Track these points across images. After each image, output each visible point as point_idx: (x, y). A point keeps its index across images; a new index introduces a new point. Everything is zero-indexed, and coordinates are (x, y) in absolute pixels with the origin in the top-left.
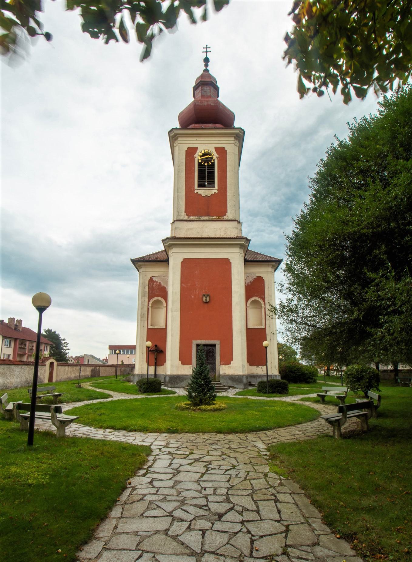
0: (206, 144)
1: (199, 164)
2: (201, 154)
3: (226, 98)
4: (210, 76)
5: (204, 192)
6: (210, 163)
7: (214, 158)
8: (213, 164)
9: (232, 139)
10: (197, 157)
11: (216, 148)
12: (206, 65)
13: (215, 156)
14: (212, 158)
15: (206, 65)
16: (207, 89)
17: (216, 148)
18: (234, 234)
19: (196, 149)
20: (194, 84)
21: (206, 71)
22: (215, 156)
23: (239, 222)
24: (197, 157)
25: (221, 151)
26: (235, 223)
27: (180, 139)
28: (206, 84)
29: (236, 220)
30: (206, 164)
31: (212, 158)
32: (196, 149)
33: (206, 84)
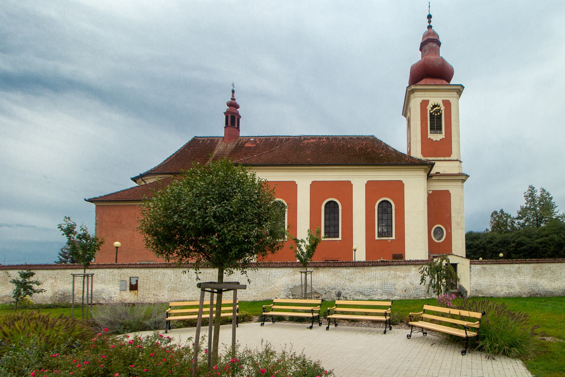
0: (436, 98)
1: (431, 114)
2: (431, 106)
3: (447, 54)
4: (434, 34)
5: (436, 137)
6: (439, 114)
7: (442, 109)
8: (441, 115)
9: (455, 93)
10: (429, 108)
11: (443, 101)
12: (430, 22)
13: (443, 108)
14: (440, 109)
15: (430, 22)
16: (431, 44)
17: (443, 101)
18: (456, 172)
19: (428, 101)
20: (420, 41)
21: (430, 27)
22: (443, 108)
23: (460, 161)
24: (429, 108)
25: (447, 104)
26: (458, 162)
27: (415, 93)
28: (431, 42)
29: (457, 160)
30: (436, 115)
31: (440, 109)
32: (428, 101)
33: (431, 42)
